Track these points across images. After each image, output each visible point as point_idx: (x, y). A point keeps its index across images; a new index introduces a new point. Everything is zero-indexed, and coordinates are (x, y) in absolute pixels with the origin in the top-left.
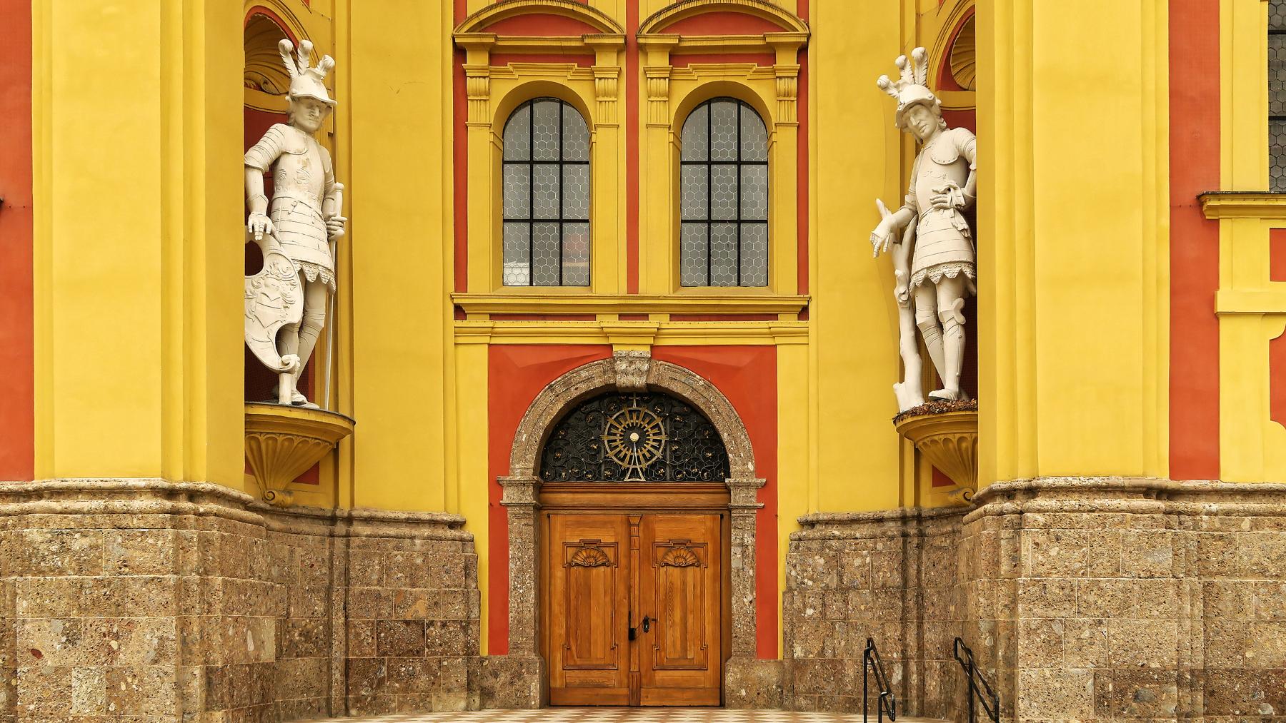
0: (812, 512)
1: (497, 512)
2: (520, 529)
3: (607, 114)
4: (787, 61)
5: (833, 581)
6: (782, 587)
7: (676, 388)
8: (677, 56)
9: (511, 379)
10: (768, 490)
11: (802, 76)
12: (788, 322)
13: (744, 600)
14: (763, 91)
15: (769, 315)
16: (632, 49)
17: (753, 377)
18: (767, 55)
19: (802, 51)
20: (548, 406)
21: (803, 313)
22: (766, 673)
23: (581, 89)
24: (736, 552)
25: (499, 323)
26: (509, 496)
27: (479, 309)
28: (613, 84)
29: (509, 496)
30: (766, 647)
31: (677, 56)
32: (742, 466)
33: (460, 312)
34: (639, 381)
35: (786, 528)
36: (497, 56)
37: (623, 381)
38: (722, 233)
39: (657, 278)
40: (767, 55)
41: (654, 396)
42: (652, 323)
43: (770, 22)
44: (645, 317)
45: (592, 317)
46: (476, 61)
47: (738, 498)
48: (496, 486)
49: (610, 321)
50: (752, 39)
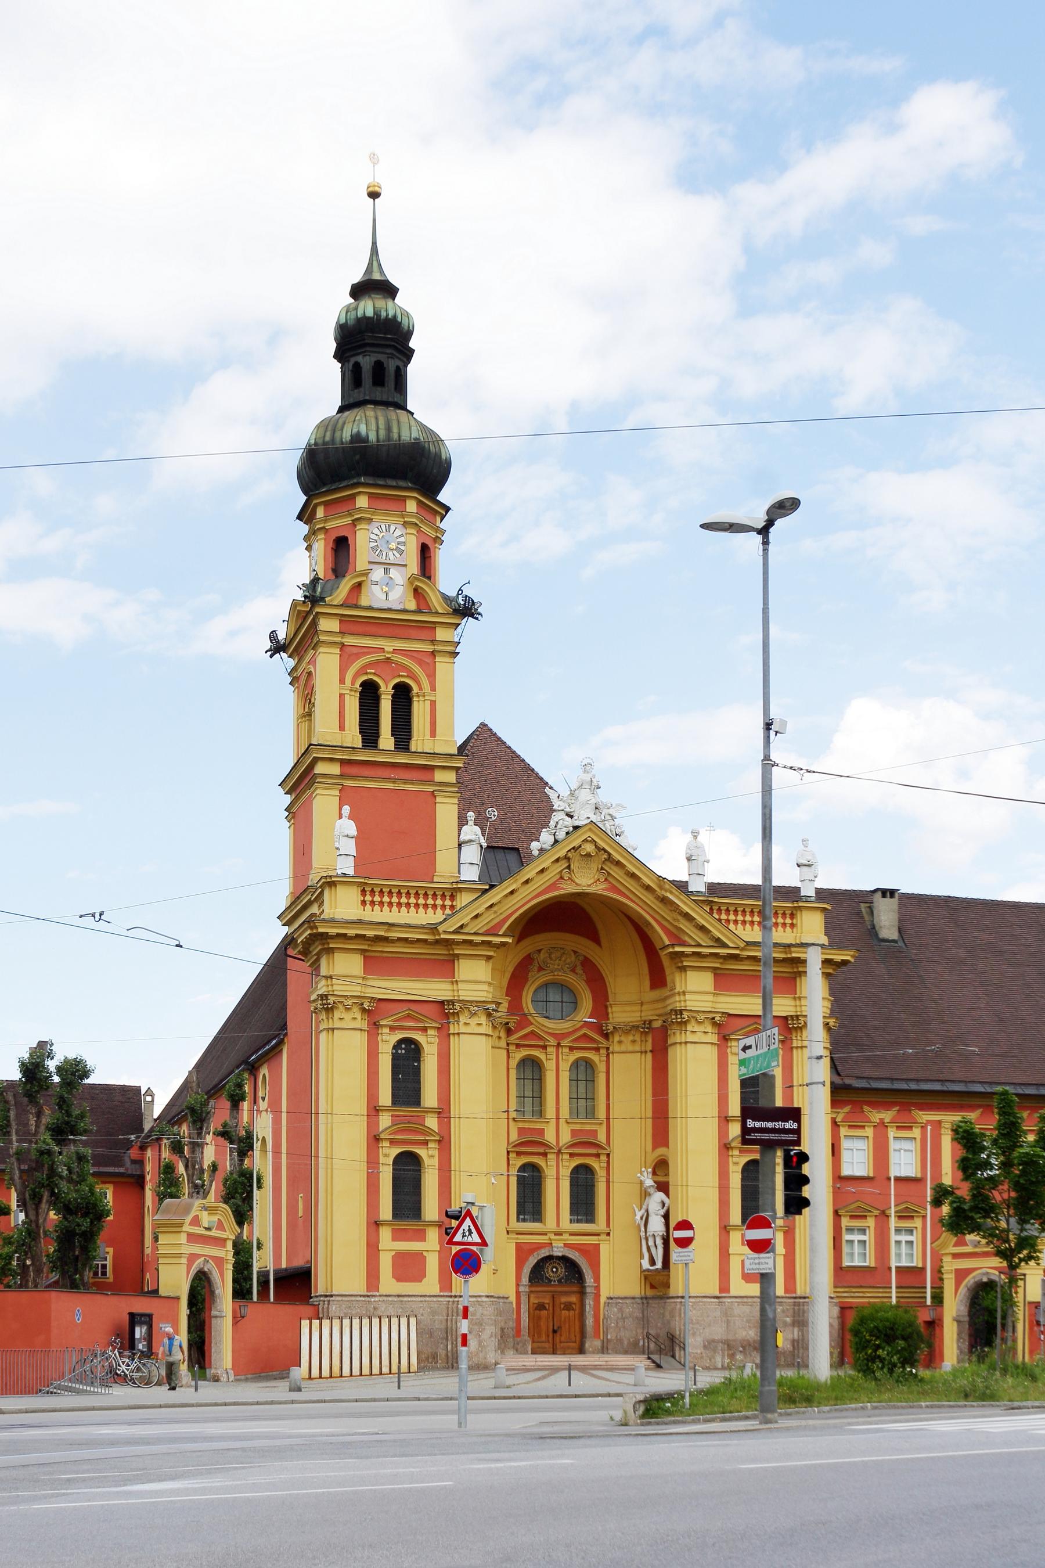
0: (612, 1295)
1: (518, 1293)
2: (524, 1299)
4: (603, 1158)
5: (620, 1315)
6: (602, 1317)
8: (571, 1155)
9: (522, 1252)
10: (598, 1288)
11: (608, 1163)
12: (603, 1237)
13: (590, 1321)
15: (598, 1235)
16: (559, 1152)
17: (592, 1253)
18: (598, 1156)
19: (608, 1155)
20: (532, 1261)
21: (608, 1234)
22: (598, 1343)
24: (588, 1307)
25: (520, 1237)
26: (521, 1289)
27: (513, 1232)
29: (521, 1289)
30: (597, 1334)
31: (571, 1155)
32: (589, 1281)
33: (508, 1232)
34: (560, 1254)
35: (603, 1300)
36: (519, 1154)
37: (555, 1254)
40: (598, 1156)
41: (564, 1259)
42: (566, 1236)
44: (561, 1234)
46: (511, 1155)
47: (588, 1290)
48: (518, 1285)
49: (553, 1237)
50: (593, 1151)
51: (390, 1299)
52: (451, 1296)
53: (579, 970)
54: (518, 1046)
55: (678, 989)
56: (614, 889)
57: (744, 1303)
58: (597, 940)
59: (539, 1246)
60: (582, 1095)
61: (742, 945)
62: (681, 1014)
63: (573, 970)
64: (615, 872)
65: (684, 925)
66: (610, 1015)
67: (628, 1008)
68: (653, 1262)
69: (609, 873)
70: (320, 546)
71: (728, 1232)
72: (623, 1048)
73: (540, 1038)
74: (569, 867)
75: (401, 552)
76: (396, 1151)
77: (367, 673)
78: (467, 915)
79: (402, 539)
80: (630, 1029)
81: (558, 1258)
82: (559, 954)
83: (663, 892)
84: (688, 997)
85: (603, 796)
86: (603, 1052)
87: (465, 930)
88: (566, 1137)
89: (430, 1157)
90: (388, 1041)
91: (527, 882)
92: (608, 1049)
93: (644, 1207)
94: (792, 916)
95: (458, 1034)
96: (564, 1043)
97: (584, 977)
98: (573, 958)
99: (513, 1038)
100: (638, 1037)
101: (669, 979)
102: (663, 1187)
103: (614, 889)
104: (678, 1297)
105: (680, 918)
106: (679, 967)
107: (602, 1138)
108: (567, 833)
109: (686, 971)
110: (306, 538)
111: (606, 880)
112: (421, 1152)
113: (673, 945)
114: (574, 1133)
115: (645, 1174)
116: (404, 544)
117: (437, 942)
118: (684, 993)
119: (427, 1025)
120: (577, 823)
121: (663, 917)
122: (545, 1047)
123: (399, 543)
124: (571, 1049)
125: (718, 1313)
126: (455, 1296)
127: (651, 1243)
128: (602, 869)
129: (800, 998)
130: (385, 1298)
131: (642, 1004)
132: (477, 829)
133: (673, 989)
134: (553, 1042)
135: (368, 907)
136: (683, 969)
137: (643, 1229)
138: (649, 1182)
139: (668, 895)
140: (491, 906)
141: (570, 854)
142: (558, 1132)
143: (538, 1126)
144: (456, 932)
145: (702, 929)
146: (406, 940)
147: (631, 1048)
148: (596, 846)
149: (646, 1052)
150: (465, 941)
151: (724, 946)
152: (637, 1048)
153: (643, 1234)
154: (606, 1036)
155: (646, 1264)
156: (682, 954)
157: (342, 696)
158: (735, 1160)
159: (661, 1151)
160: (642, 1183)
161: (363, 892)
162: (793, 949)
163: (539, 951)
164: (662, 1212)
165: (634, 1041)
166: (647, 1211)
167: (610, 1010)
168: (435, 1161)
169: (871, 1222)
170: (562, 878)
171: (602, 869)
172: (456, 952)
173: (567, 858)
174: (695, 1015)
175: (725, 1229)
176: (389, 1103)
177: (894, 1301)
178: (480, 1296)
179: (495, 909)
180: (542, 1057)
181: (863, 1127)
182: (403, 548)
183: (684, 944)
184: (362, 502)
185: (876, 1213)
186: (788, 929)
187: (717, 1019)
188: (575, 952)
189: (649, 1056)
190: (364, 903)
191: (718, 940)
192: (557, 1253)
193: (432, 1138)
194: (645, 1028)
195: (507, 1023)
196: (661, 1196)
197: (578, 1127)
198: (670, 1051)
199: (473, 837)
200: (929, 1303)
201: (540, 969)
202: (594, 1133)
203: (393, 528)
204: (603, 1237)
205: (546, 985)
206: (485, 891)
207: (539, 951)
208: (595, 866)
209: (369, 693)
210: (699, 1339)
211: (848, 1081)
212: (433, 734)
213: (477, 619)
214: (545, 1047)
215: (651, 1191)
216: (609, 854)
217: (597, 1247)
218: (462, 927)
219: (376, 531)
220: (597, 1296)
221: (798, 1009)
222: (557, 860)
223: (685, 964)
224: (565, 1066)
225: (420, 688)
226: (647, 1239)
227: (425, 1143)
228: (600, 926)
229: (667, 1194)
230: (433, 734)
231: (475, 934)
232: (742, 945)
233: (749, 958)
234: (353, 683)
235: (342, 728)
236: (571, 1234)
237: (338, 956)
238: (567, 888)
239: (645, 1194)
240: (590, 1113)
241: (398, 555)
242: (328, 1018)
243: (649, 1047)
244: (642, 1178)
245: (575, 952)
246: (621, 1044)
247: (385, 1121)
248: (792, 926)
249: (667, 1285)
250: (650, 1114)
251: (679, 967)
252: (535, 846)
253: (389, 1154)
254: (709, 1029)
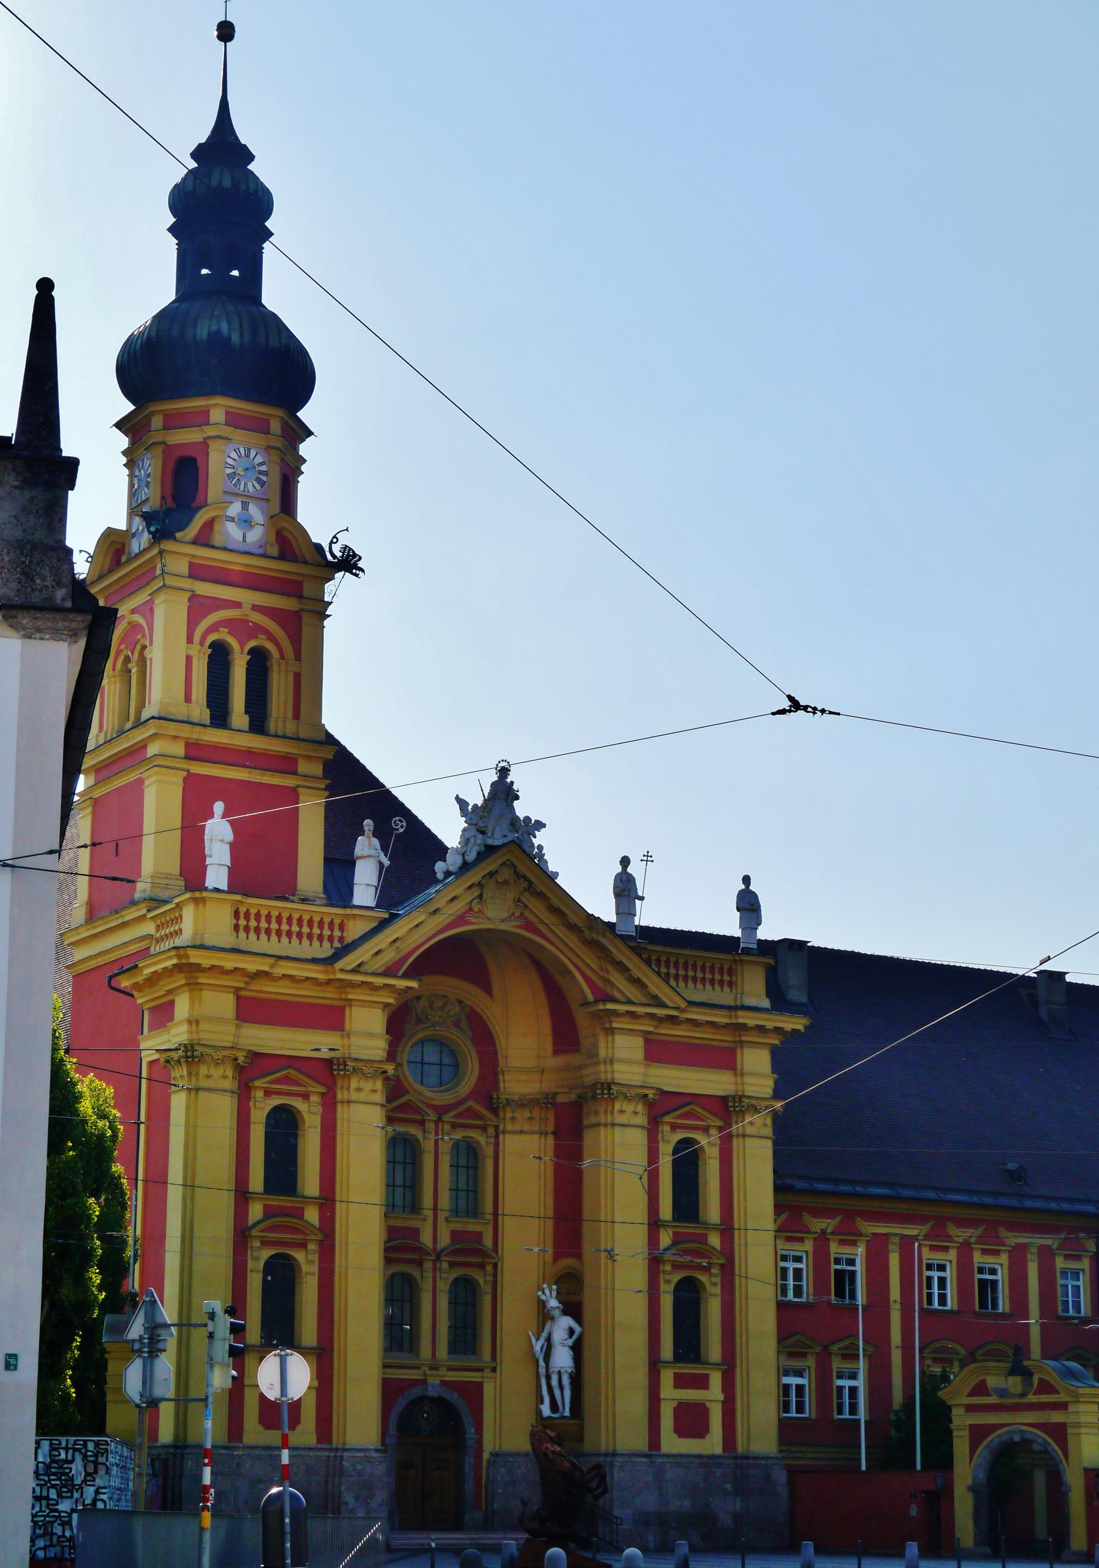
3: (427, 1285)
4: (489, 1268)
6: (484, 1480)
7: (448, 1397)
8: (452, 1265)
9: (390, 1390)
10: (480, 1441)
11: (495, 1275)
12: (487, 1373)
13: (469, 1485)
14: (480, 1279)
17: (473, 1393)
18: (482, 1266)
19: (495, 1265)
20: (402, 1403)
21: (494, 1370)
23: (416, 1274)
24: (467, 1466)
26: (388, 1441)
28: (429, 1274)
31: (452, 1265)
34: (436, 1395)
35: (486, 1456)
38: (465, 1335)
39: (443, 1352)
40: (482, 1266)
41: (440, 1402)
42: (443, 1371)
43: (483, 1253)
44: (437, 1369)
45: (418, 1368)
49: (428, 1372)
51: (257, 1452)
52: (331, 1450)
53: (464, 1024)
55: (602, 1054)
56: (530, 927)
57: (678, 1465)
58: (488, 989)
59: (414, 1383)
60: (462, 1185)
61: (683, 1005)
62: (609, 1089)
63: (457, 1025)
64: (536, 907)
65: (615, 977)
66: (501, 1085)
67: (524, 1077)
68: (554, 1407)
69: (526, 906)
70: (152, 464)
71: (658, 1371)
72: (518, 1128)
73: (417, 1110)
74: (480, 897)
75: (262, 484)
76: (266, 1253)
77: (217, 631)
78: (367, 952)
79: (264, 468)
80: (524, 1103)
81: (432, 1400)
82: (440, 1004)
83: (594, 936)
84: (617, 1067)
85: (521, 809)
86: (491, 1131)
87: (362, 969)
88: (444, 1240)
89: (307, 1262)
90: (261, 1109)
91: (435, 912)
92: (497, 1127)
93: (544, 1335)
94: (730, 972)
95: (349, 1102)
96: (448, 1117)
97: (470, 1034)
98: (457, 1009)
100: (536, 1114)
101: (585, 1042)
102: (573, 1309)
103: (530, 927)
104: (599, 1455)
105: (609, 967)
106: (605, 1029)
107: (488, 1242)
108: (479, 853)
109: (613, 1034)
110: (124, 453)
111: (522, 914)
112: (299, 1256)
113: (597, 1001)
114: (454, 1233)
115: (547, 1292)
116: (265, 473)
117: (329, 982)
118: (612, 1063)
119: (310, 1089)
120: (490, 842)
121: (587, 965)
122: (422, 1123)
123: (260, 472)
124: (454, 1126)
125: (650, 1478)
126: (337, 1449)
127: (554, 1382)
128: (519, 900)
129: (742, 1075)
130: (251, 1452)
131: (543, 1072)
132: (376, 842)
133: (593, 1054)
134: (433, 1116)
135: (242, 934)
136: (612, 1031)
137: (542, 1363)
138: (553, 1303)
139: (600, 938)
140: (394, 941)
141: (484, 882)
142: (435, 1231)
143: (413, 1224)
144: (355, 971)
145: (638, 982)
146: (291, 978)
147: (526, 1128)
148: (516, 873)
149: (546, 1134)
150: (364, 983)
151: (663, 1005)
152: (536, 1128)
153: (542, 1371)
154: (495, 1111)
155: (546, 1410)
156: (615, 1013)
157: (189, 659)
158: (668, 1277)
159: (568, 1262)
160: (542, 1304)
161: (236, 914)
162: (740, 1013)
164: (570, 1342)
165: (531, 1119)
166: (549, 1340)
167: (501, 1077)
168: (315, 1269)
169: (811, 1362)
170: (471, 909)
172: (350, 996)
173: (480, 885)
174: (624, 1090)
175: (655, 1365)
176: (261, 1189)
177: (864, 1468)
178: (367, 1450)
179: (397, 944)
181: (801, 1240)
182: (264, 478)
183: (614, 1000)
184: (217, 415)
185: (818, 1349)
186: (726, 989)
187: (651, 1096)
189: (551, 1140)
190: (236, 928)
191: (655, 997)
192: (432, 1393)
193: (314, 1238)
194: (547, 1101)
196: (567, 1321)
197: (459, 1227)
198: (588, 1136)
199: (373, 852)
200: (864, 1468)
201: (419, 1021)
202: (479, 1236)
203: (253, 453)
204: (487, 1373)
205: (422, 1042)
206: (383, 924)
208: (511, 896)
209: (219, 657)
210: (629, 1512)
211: (788, 1181)
212: (296, 715)
213: (357, 575)
214: (422, 1123)
215: (556, 1313)
216: (530, 883)
217: (480, 1386)
218: (359, 965)
219: (234, 455)
220: (480, 1450)
221: (740, 1088)
222: (470, 887)
223: (614, 1025)
224: (446, 1146)
225: (282, 657)
226: (548, 1378)
227: (303, 1245)
228: (493, 970)
229: (579, 1320)
230: (296, 715)
231: (374, 974)
232: (683, 1005)
233: (688, 1020)
234: (202, 644)
235: (188, 699)
236: (450, 1369)
237: (207, 994)
238: (478, 924)
239: (544, 1316)
240: (473, 1211)
241: (258, 487)
242: (190, 1074)
243: (551, 1128)
244: (543, 1297)
245: (460, 1002)
246: (515, 1120)
247: (256, 1211)
248: (731, 984)
249: (580, 1439)
250: (550, 1213)
251: (605, 1029)
252: (440, 867)
253: (259, 1257)
254: (640, 1108)
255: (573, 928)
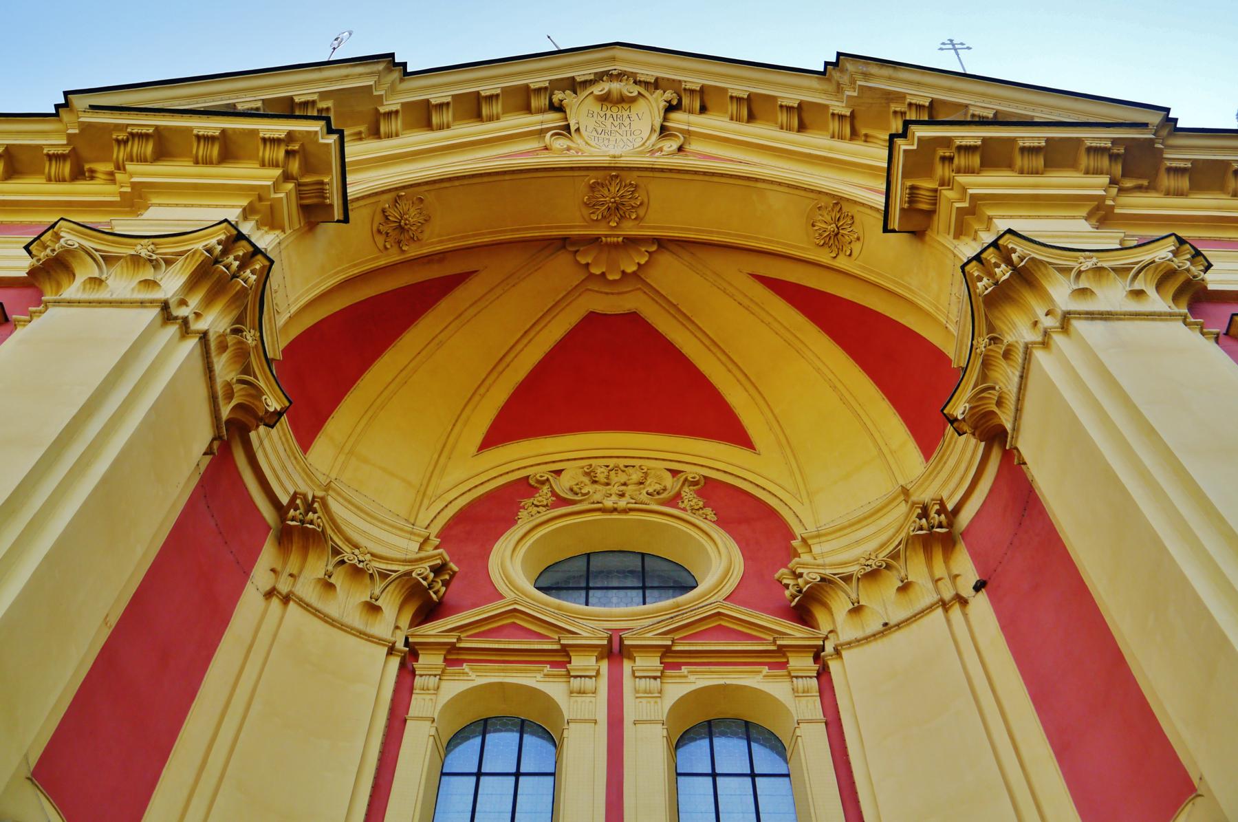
54: (454, 656)
58: (736, 434)
86: (803, 663)
99: (433, 630)
111: (680, 149)
124: (671, 659)
149: (963, 602)
152: (924, 595)
154: (802, 613)
163: (558, 473)
171: (663, 129)
180: (555, 689)
188: (674, 473)
189: (981, 604)
195: (409, 574)
207: (558, 473)
228: (736, 397)
255: (802, 117)
